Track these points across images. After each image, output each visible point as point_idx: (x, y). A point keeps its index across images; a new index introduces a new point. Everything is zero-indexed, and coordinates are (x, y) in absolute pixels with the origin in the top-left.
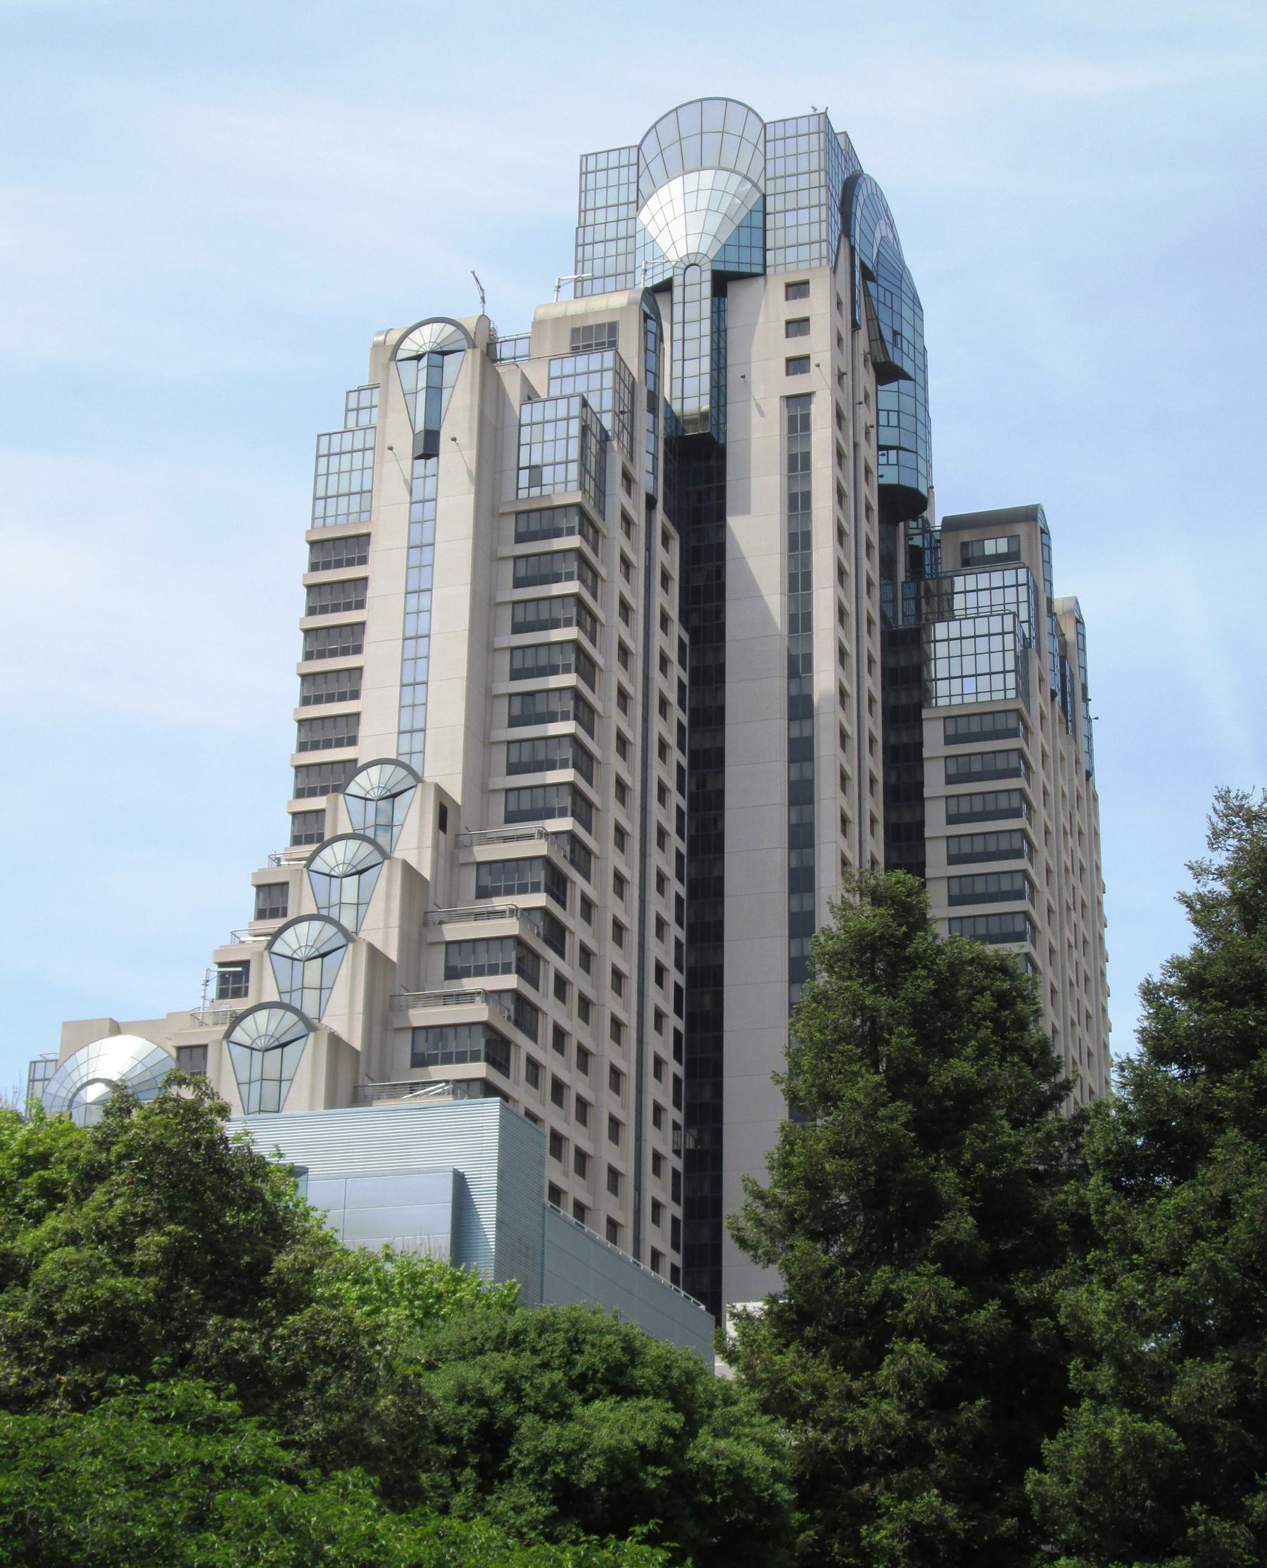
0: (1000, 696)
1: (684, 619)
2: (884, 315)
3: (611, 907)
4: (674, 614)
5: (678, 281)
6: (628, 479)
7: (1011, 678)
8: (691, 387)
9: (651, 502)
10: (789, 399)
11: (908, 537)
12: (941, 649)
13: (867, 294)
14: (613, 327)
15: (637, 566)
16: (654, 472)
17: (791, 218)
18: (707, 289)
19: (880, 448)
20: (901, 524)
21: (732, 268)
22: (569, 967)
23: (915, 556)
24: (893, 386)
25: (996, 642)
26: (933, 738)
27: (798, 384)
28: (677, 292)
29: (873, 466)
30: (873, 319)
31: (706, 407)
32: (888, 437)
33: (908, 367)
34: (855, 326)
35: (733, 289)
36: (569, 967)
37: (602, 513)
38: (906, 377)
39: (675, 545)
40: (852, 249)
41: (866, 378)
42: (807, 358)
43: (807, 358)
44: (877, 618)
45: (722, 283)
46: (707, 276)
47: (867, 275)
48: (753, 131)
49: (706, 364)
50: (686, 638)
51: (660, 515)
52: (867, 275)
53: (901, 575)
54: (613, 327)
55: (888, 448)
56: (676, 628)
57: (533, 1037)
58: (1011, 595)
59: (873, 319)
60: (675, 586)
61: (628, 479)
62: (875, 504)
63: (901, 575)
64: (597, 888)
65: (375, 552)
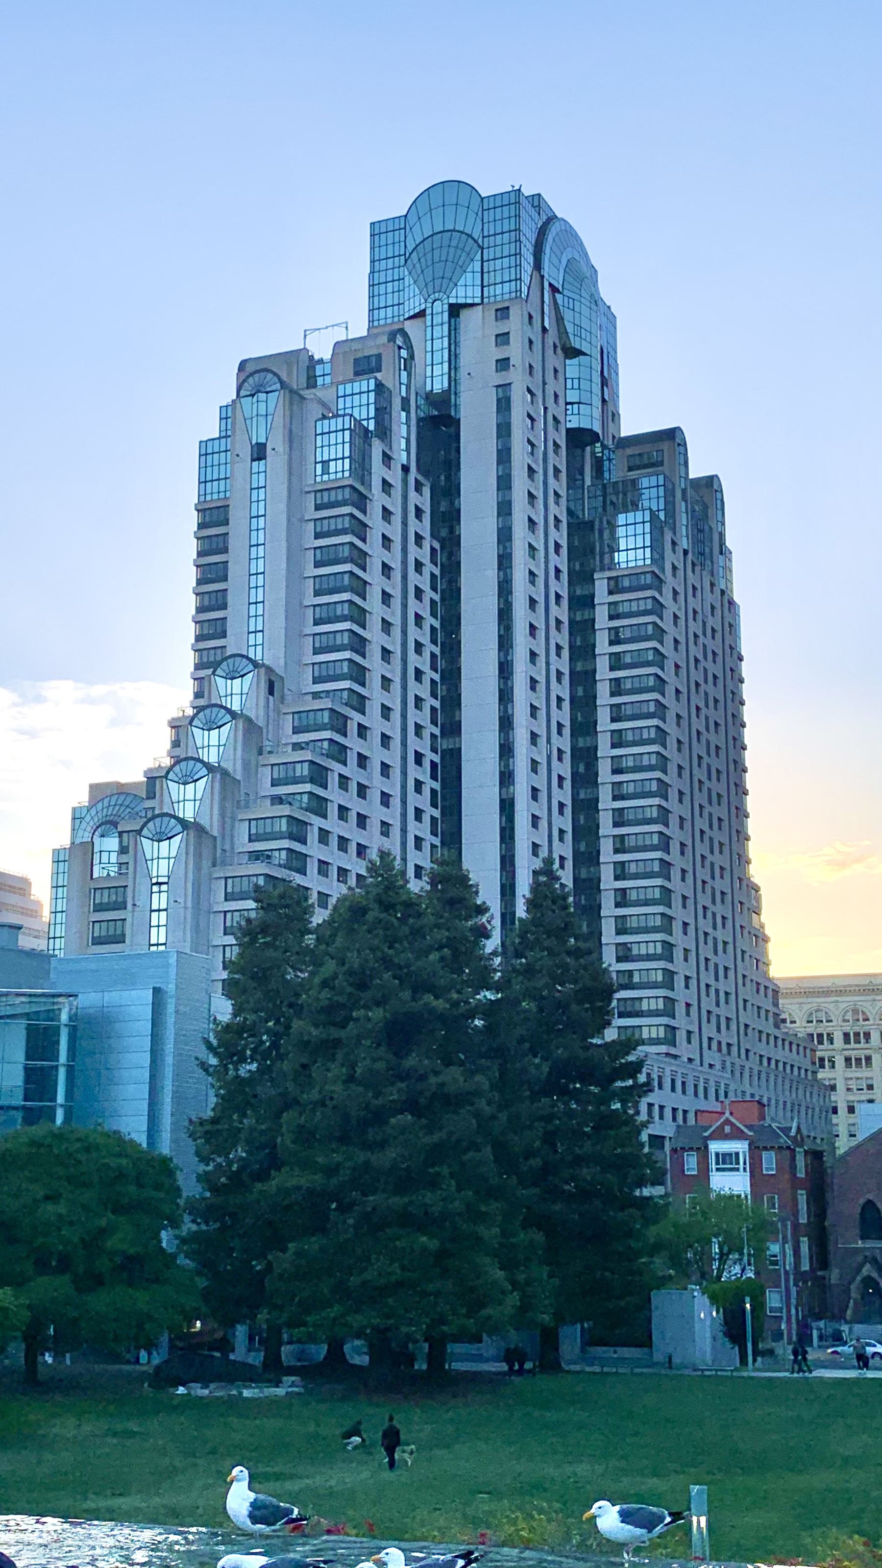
0: (641, 563)
1: (432, 536)
2: (568, 315)
4: (426, 534)
6: (387, 459)
9: (406, 469)
11: (593, 453)
14: (379, 357)
15: (396, 511)
16: (408, 450)
18: (446, 315)
19: (567, 404)
20: (588, 449)
22: (351, 770)
23: (598, 464)
24: (575, 361)
25: (639, 528)
28: (429, 318)
29: (561, 418)
32: (572, 396)
34: (544, 330)
35: (464, 314)
36: (351, 770)
38: (585, 354)
39: (427, 491)
40: (542, 277)
42: (508, 359)
43: (508, 359)
45: (455, 310)
46: (446, 307)
47: (554, 289)
48: (476, 202)
50: (437, 545)
52: (554, 289)
53: (588, 482)
54: (379, 357)
55: (572, 403)
57: (325, 816)
59: (559, 320)
61: (387, 459)
62: (563, 443)
63: (588, 482)
64: (373, 719)
65: (233, 514)
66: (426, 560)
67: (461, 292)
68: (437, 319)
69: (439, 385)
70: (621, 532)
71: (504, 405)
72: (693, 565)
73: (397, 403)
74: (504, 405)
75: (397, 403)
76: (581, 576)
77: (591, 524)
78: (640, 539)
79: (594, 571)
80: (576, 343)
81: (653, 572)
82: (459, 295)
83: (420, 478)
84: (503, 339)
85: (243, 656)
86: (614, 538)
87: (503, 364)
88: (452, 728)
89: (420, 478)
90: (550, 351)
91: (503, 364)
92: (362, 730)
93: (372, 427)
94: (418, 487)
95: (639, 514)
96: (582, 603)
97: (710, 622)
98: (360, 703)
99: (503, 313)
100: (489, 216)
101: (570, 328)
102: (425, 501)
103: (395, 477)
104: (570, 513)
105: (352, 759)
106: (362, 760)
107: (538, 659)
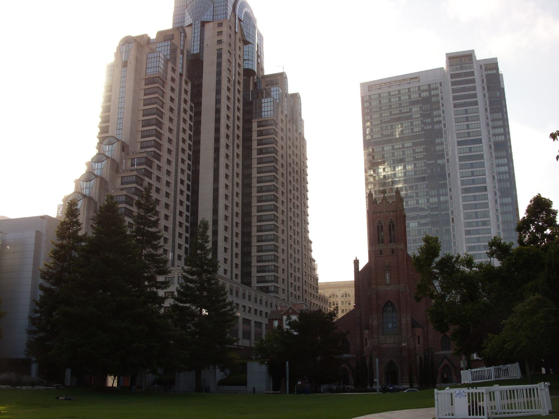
1: (192, 100)
2: (245, 29)
5: (193, 24)
8: (195, 48)
9: (181, 75)
10: (217, 50)
11: (253, 79)
17: (219, 8)
18: (200, 25)
19: (244, 60)
20: (252, 77)
21: (205, 20)
23: (255, 84)
26: (255, 125)
29: (241, 64)
31: (198, 51)
32: (246, 57)
33: (251, 41)
38: (251, 43)
39: (189, 84)
40: (236, 15)
41: (239, 44)
44: (241, 99)
45: (203, 24)
46: (200, 22)
49: (199, 43)
50: (193, 105)
52: (240, 20)
53: (251, 89)
56: (189, 103)
59: (242, 30)
61: (174, 70)
62: (242, 73)
63: (251, 89)
66: (188, 109)
67: (205, 17)
68: (196, 26)
69: (196, 51)
70: (263, 105)
71: (219, 56)
72: (289, 121)
73: (179, 52)
74: (219, 56)
75: (179, 52)
76: (247, 122)
77: (252, 102)
78: (269, 108)
79: (252, 119)
80: (248, 39)
81: (274, 120)
82: (204, 18)
83: (187, 79)
84: (220, 33)
85: (114, 137)
86: (260, 107)
87: (220, 42)
89: (187, 79)
90: (238, 41)
91: (220, 42)
92: (159, 168)
93: (168, 58)
94: (186, 83)
95: (269, 99)
96: (247, 130)
97: (295, 143)
98: (158, 157)
99: (220, 25)
101: (245, 34)
103: (177, 77)
105: (154, 177)
106: (158, 179)
107: (231, 153)
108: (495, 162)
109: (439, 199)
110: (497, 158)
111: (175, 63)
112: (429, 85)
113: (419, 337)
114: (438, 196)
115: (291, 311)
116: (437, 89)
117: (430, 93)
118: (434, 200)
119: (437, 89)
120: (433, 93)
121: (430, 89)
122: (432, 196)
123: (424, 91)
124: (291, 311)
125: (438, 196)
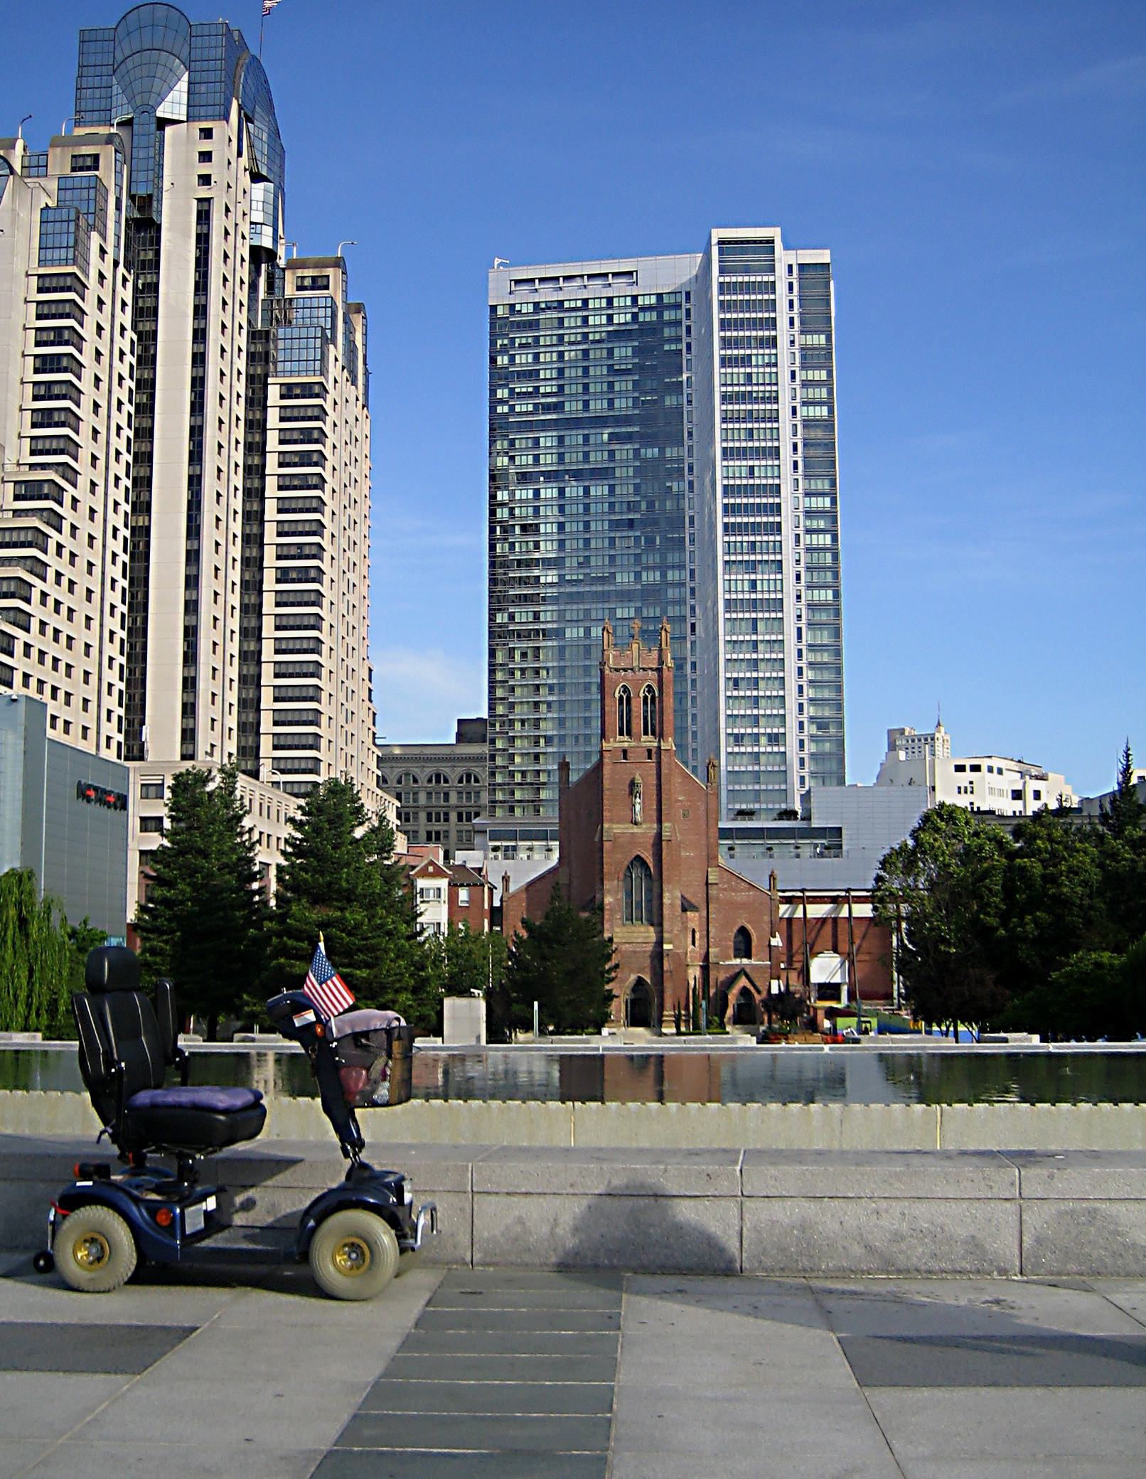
1: (134, 328)
3: (86, 500)
4: (128, 325)
6: (103, 251)
7: (318, 363)
9: (116, 264)
12: (281, 344)
13: (248, 131)
19: (252, 223)
26: (273, 393)
27: (204, 192)
30: (251, 146)
34: (240, 154)
35: (169, 130)
36: (64, 538)
37: (87, 276)
44: (245, 325)
50: (135, 338)
51: (121, 270)
58: (322, 312)
60: (129, 309)
61: (103, 251)
62: (247, 258)
63: (262, 294)
88: (142, 507)
100: (197, 42)
102: (127, 294)
104: (249, 322)
108: (806, 503)
109: (663, 576)
110: (808, 494)
111: (104, 238)
112: (660, 296)
113: (694, 931)
114: (663, 569)
115: (431, 869)
116: (677, 306)
117: (660, 315)
118: (651, 577)
119: (677, 306)
120: (667, 315)
121: (661, 304)
122: (647, 568)
123: (644, 309)
124: (431, 869)
125: (663, 569)
